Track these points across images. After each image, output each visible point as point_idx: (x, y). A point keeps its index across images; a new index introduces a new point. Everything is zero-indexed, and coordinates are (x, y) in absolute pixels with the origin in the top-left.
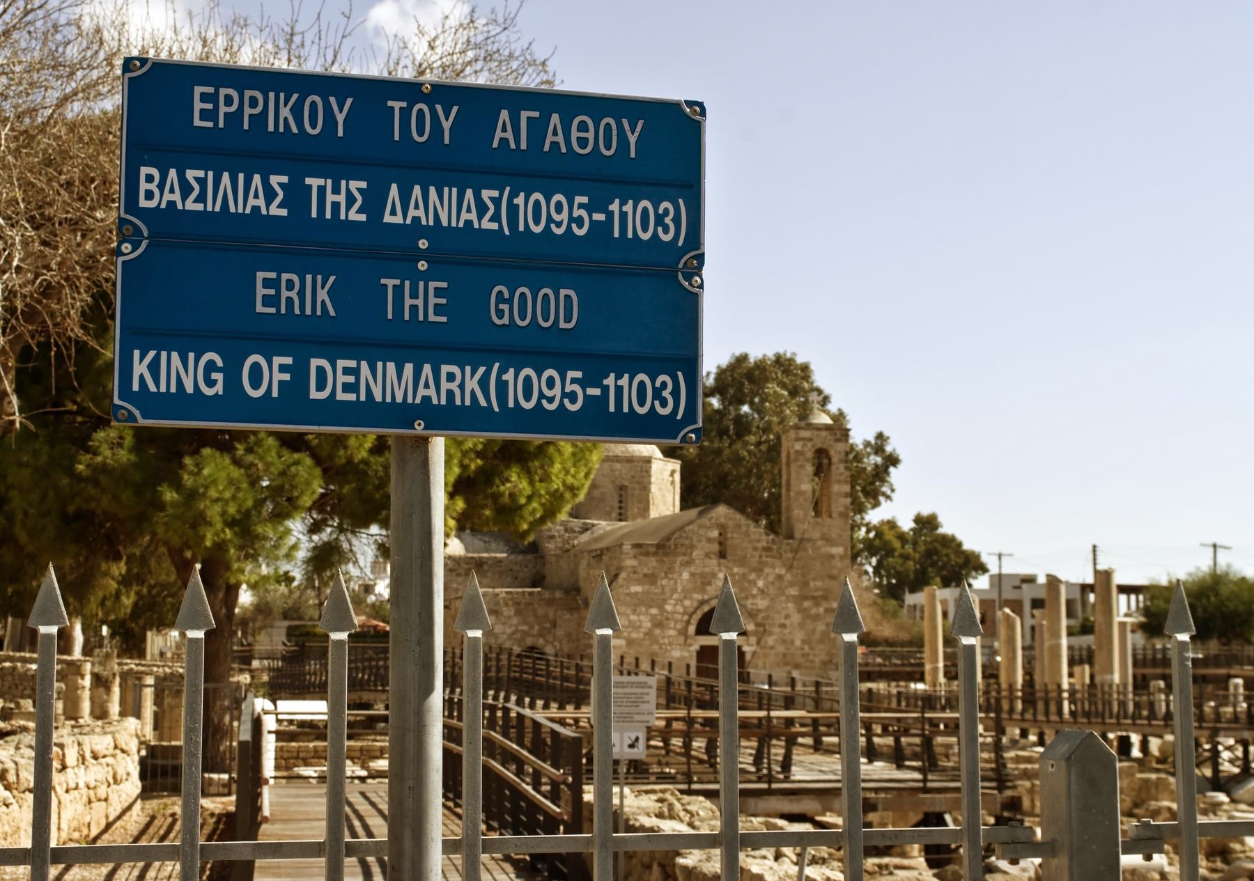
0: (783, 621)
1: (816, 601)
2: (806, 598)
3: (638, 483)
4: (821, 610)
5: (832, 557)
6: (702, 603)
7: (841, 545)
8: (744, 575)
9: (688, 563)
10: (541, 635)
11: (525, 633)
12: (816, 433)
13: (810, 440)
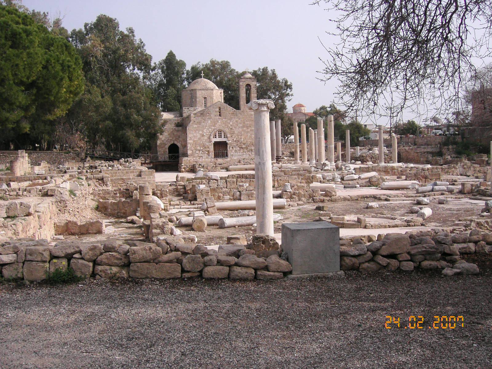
1: (247, 127)
2: (243, 127)
4: (249, 130)
6: (214, 129)
8: (226, 122)
10: (176, 140)
11: (171, 140)
13: (245, 81)
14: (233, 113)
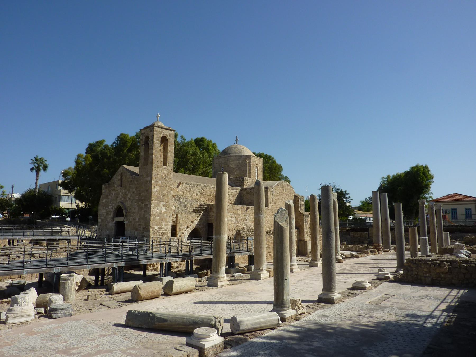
5: (147, 181)
9: (114, 190)
14: (131, 181)
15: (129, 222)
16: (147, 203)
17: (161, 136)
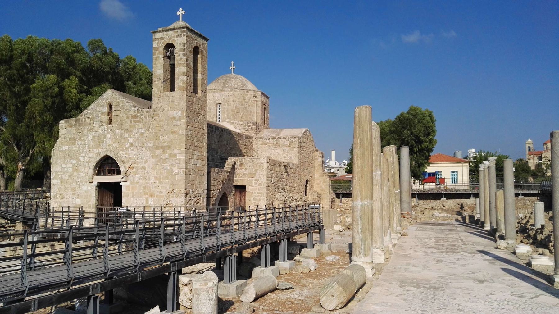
0: (144, 165)
2: (157, 148)
3: (226, 102)
5: (174, 118)
6: (98, 154)
7: (180, 109)
12: (165, 33)
13: (162, 38)
14: (135, 117)
15: (131, 183)
16: (175, 152)
17: (194, 46)
